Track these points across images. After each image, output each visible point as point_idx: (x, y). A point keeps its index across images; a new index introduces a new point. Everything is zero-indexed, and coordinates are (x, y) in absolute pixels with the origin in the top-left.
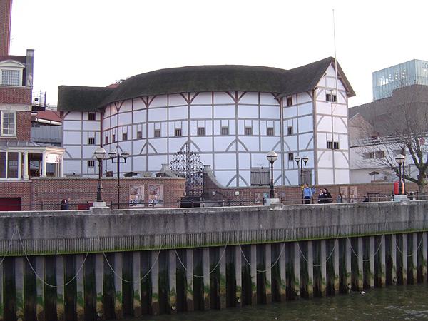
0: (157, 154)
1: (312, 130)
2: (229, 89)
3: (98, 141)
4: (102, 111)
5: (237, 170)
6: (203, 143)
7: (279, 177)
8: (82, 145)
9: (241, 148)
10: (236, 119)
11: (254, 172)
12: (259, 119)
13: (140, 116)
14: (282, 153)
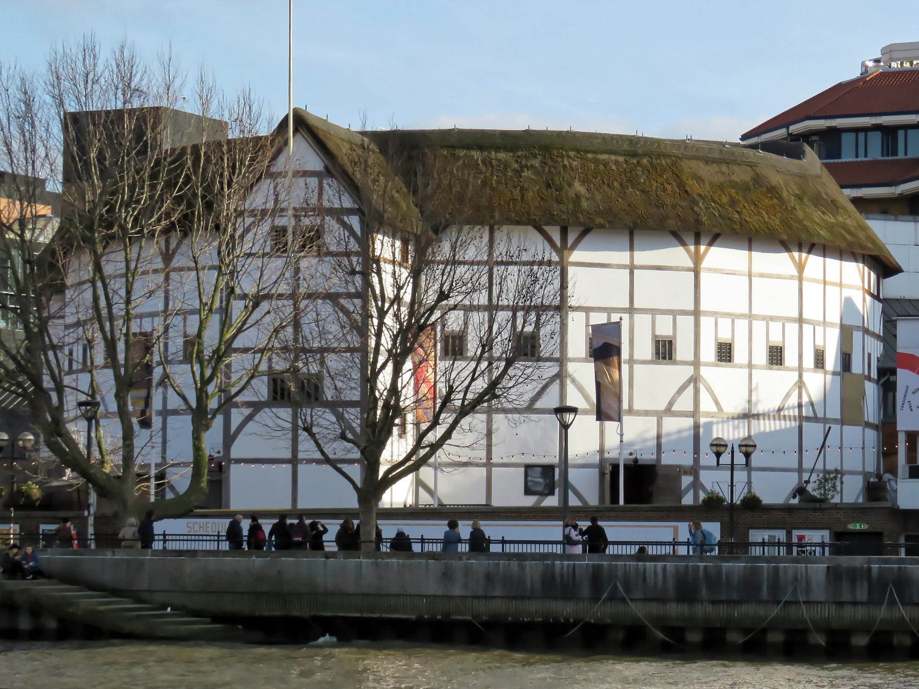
12: (750, 317)
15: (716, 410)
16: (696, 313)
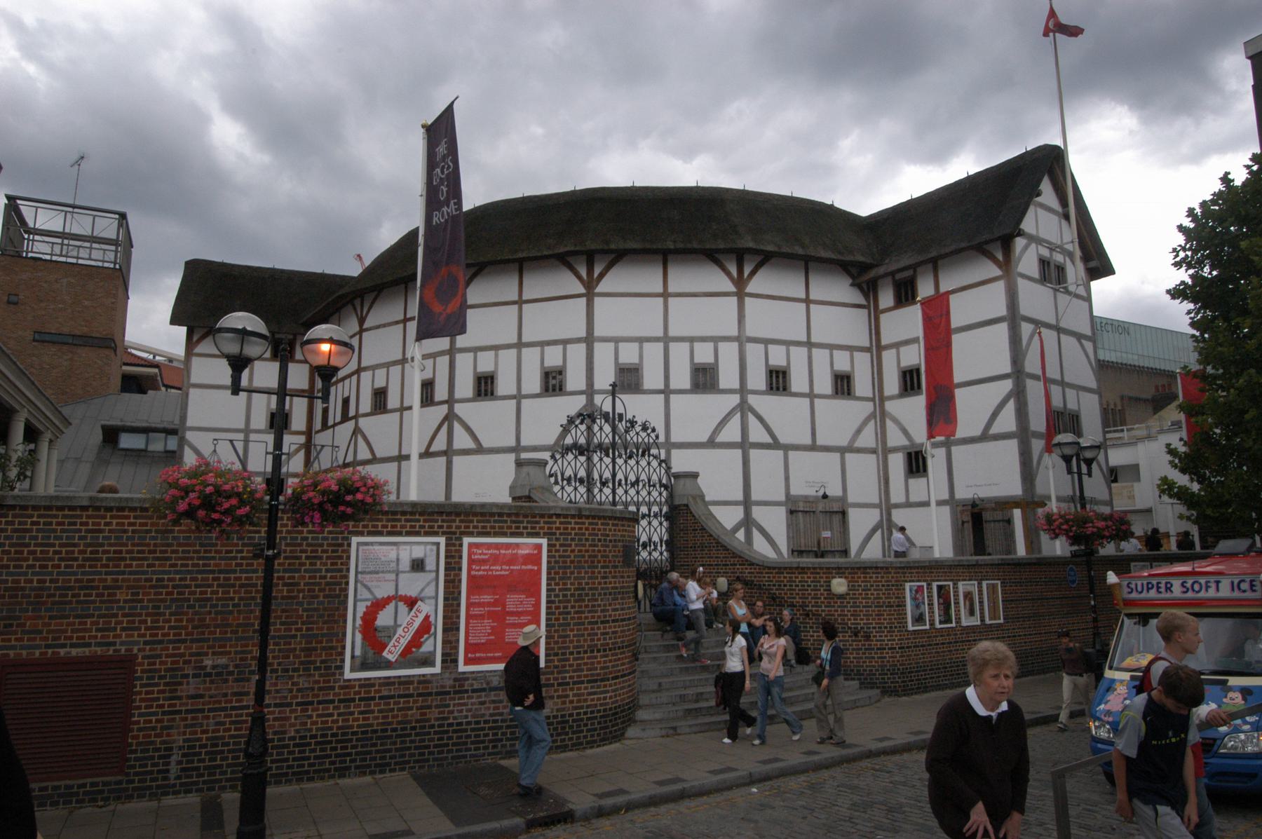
0: (480, 450)
1: (1007, 369)
5: (747, 503)
7: (873, 531)
9: (757, 434)
10: (741, 340)
11: (797, 509)
12: (809, 344)
14: (882, 451)
15: (769, 440)
16: (741, 340)
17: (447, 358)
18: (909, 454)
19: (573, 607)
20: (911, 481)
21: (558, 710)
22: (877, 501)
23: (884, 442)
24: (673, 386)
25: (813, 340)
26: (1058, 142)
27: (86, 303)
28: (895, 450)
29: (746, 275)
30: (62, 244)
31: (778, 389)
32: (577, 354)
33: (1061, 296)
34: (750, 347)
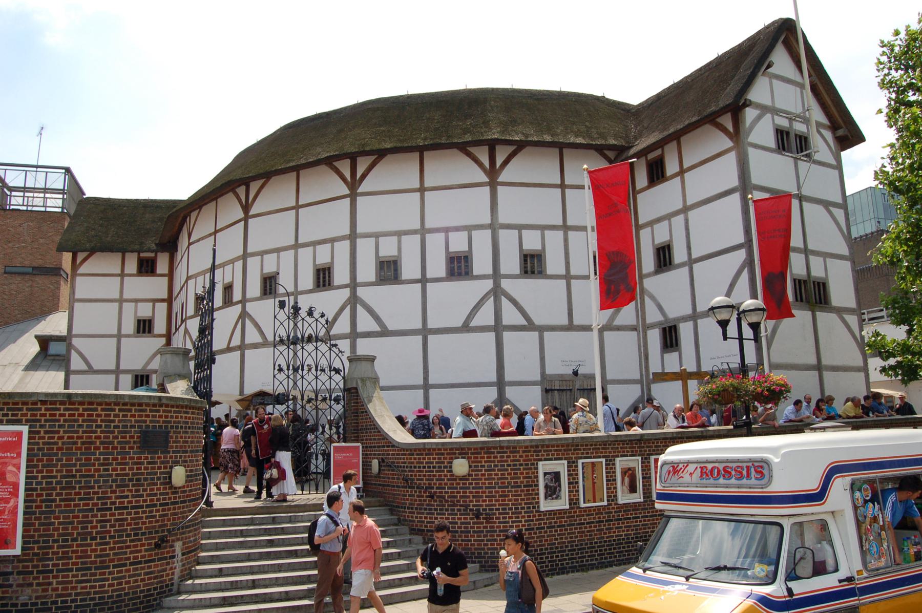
2: (468, 138)
3: (160, 326)
4: (170, 246)
5: (501, 384)
6: (396, 304)
8: (119, 336)
9: (511, 316)
10: (494, 227)
12: (565, 228)
13: (230, 244)
15: (525, 323)
17: (239, 264)
18: (664, 330)
19: (57, 495)
20: (666, 356)
21: (37, 598)
22: (638, 377)
23: (644, 319)
24: (429, 276)
25: (569, 223)
26: (794, 18)
27: (41, 241)
28: (652, 326)
29: (498, 165)
30: (24, 197)
31: (533, 272)
32: (343, 248)
33: (803, 166)
34: (502, 233)
